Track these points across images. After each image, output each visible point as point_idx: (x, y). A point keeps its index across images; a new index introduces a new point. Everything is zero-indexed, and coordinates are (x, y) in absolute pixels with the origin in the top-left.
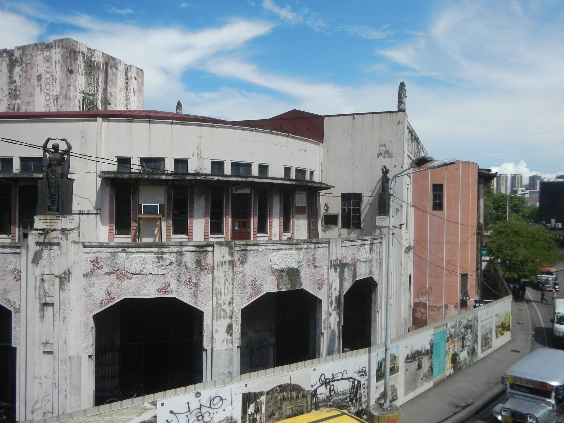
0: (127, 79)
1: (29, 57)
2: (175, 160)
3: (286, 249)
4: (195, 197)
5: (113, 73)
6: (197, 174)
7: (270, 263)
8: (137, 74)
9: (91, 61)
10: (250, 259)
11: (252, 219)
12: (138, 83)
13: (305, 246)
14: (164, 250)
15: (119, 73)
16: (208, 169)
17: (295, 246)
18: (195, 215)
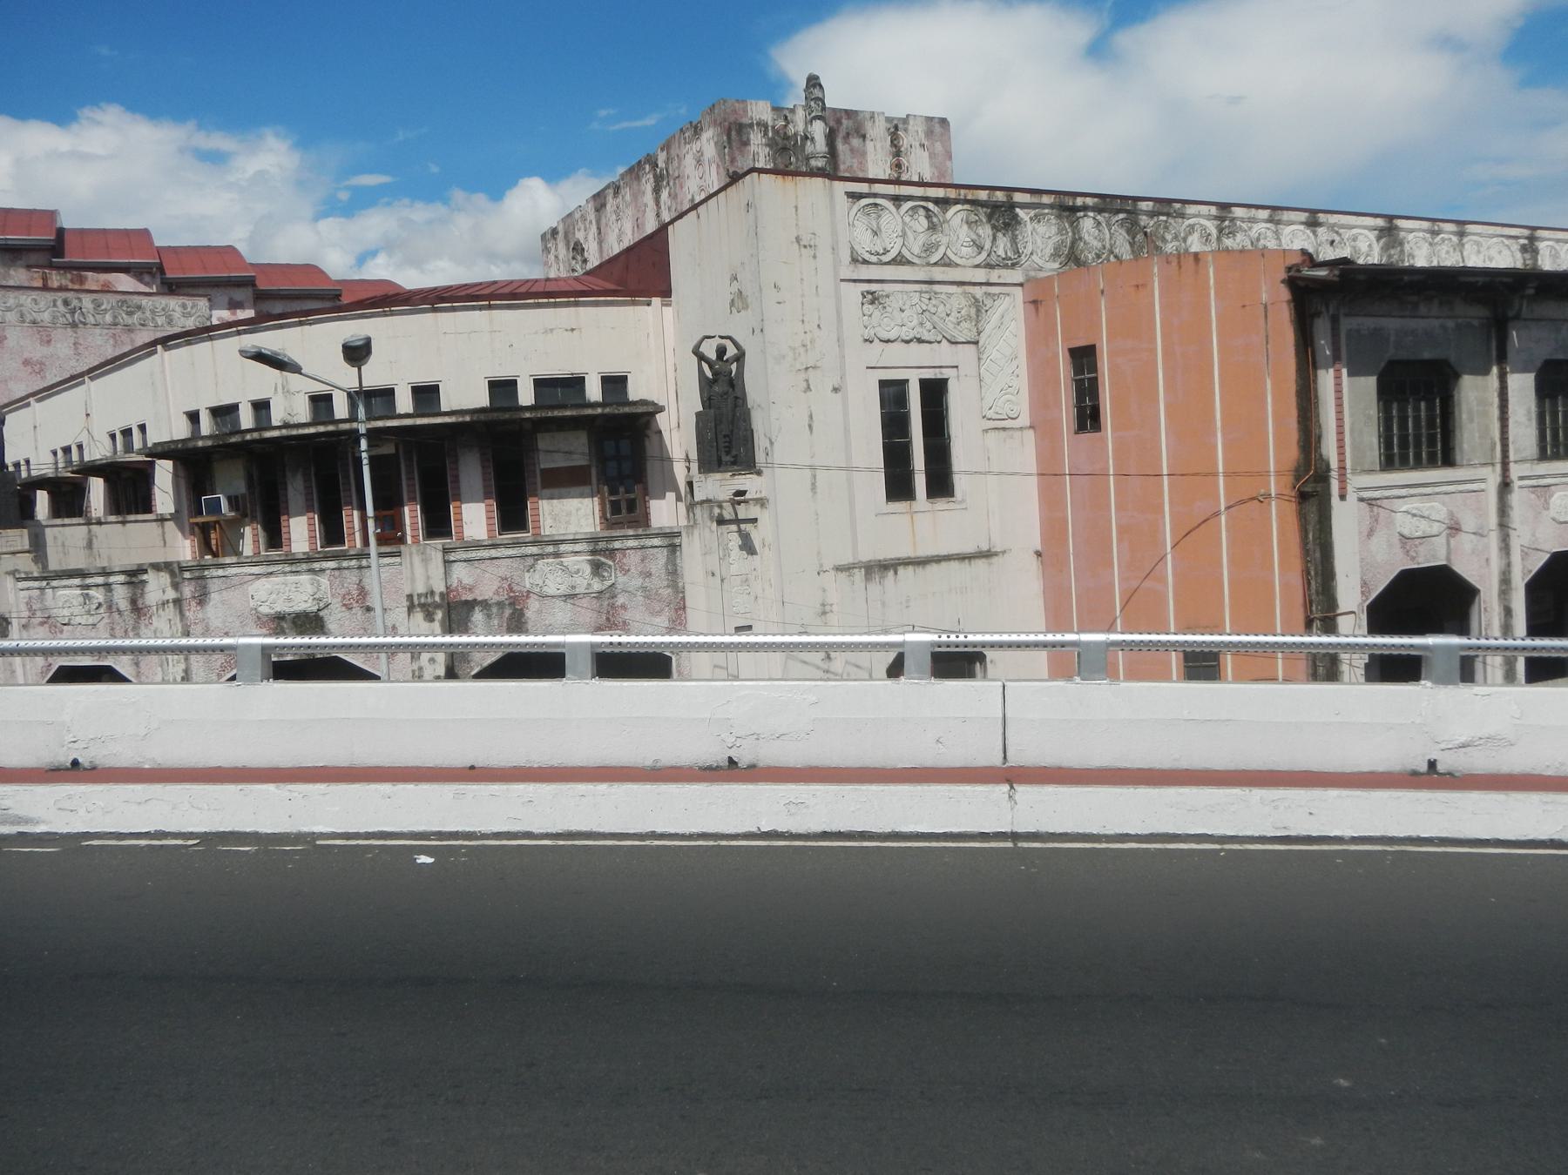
0: (897, 154)
1: (676, 163)
2: (490, 383)
3: (285, 573)
4: (289, 474)
5: (852, 150)
6: (286, 426)
7: (252, 604)
8: (929, 133)
9: (786, 137)
10: (215, 597)
11: (406, 509)
12: (932, 156)
13: (332, 564)
14: (89, 581)
15: (869, 145)
16: (303, 413)
17: (304, 566)
18: (292, 506)
